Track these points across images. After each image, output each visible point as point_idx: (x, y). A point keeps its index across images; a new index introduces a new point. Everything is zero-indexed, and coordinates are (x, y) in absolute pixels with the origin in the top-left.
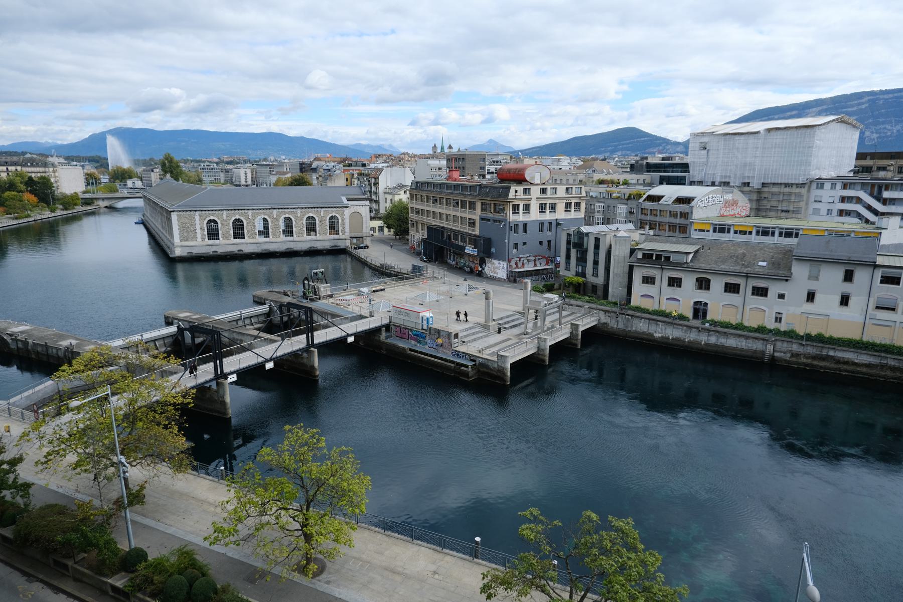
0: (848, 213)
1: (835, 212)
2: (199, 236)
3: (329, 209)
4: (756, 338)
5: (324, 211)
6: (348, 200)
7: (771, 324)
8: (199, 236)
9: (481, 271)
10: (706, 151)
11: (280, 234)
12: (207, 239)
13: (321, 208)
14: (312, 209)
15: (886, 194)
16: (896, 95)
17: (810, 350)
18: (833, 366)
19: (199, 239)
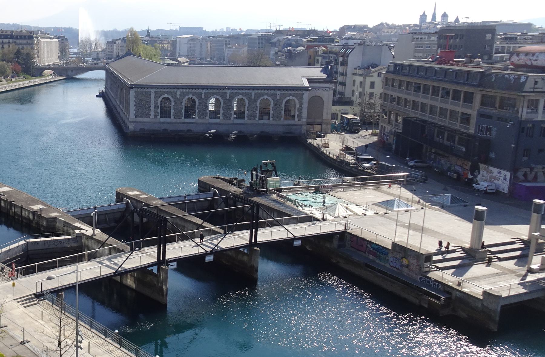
2: (152, 113)
8: (152, 113)
9: (472, 179)
12: (159, 117)
19: (152, 117)
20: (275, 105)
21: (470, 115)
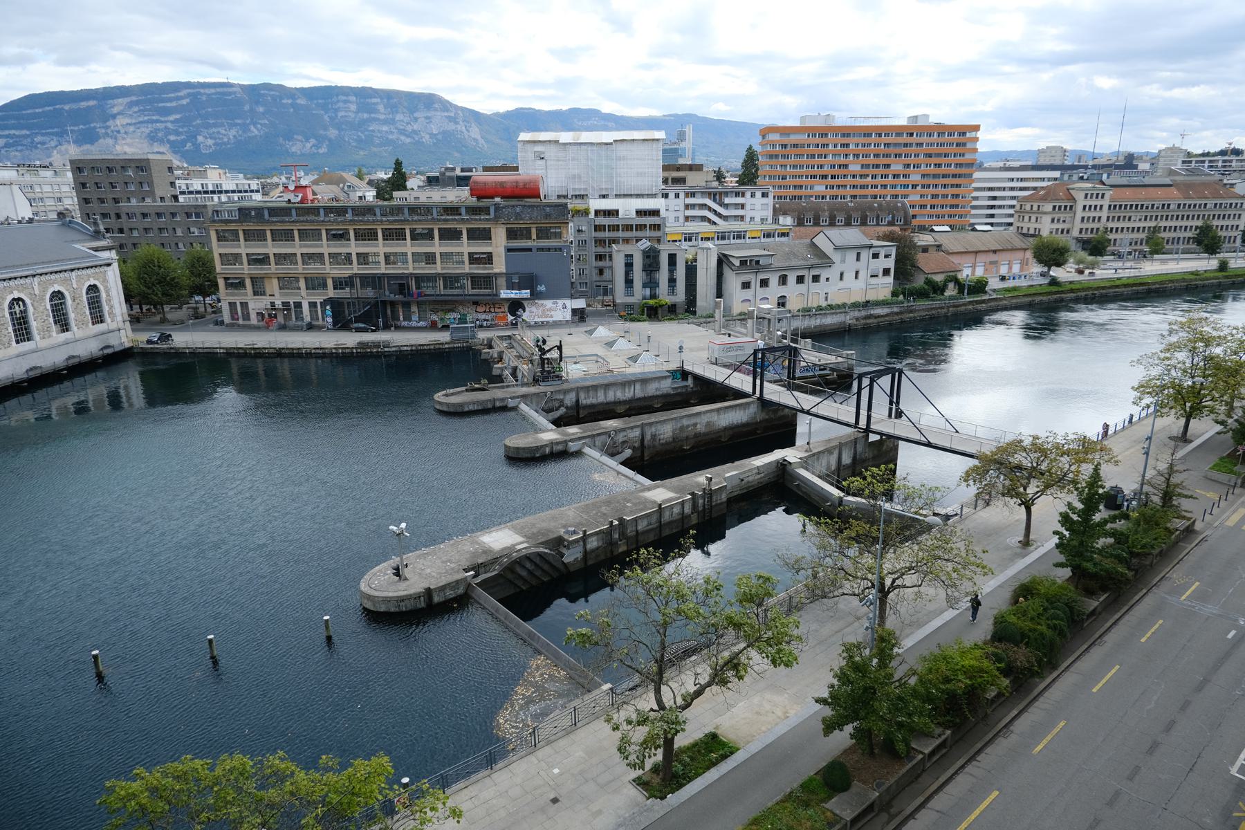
0: (693, 218)
1: (682, 219)
3: (84, 272)
4: (841, 313)
5: (77, 276)
6: (96, 249)
7: (824, 304)
10: (544, 160)
11: (10, 340)
13: (72, 270)
14: (57, 276)
15: (727, 201)
16: (218, 90)
17: (863, 313)
18: (875, 321)
20: (74, 301)
21: (491, 253)
